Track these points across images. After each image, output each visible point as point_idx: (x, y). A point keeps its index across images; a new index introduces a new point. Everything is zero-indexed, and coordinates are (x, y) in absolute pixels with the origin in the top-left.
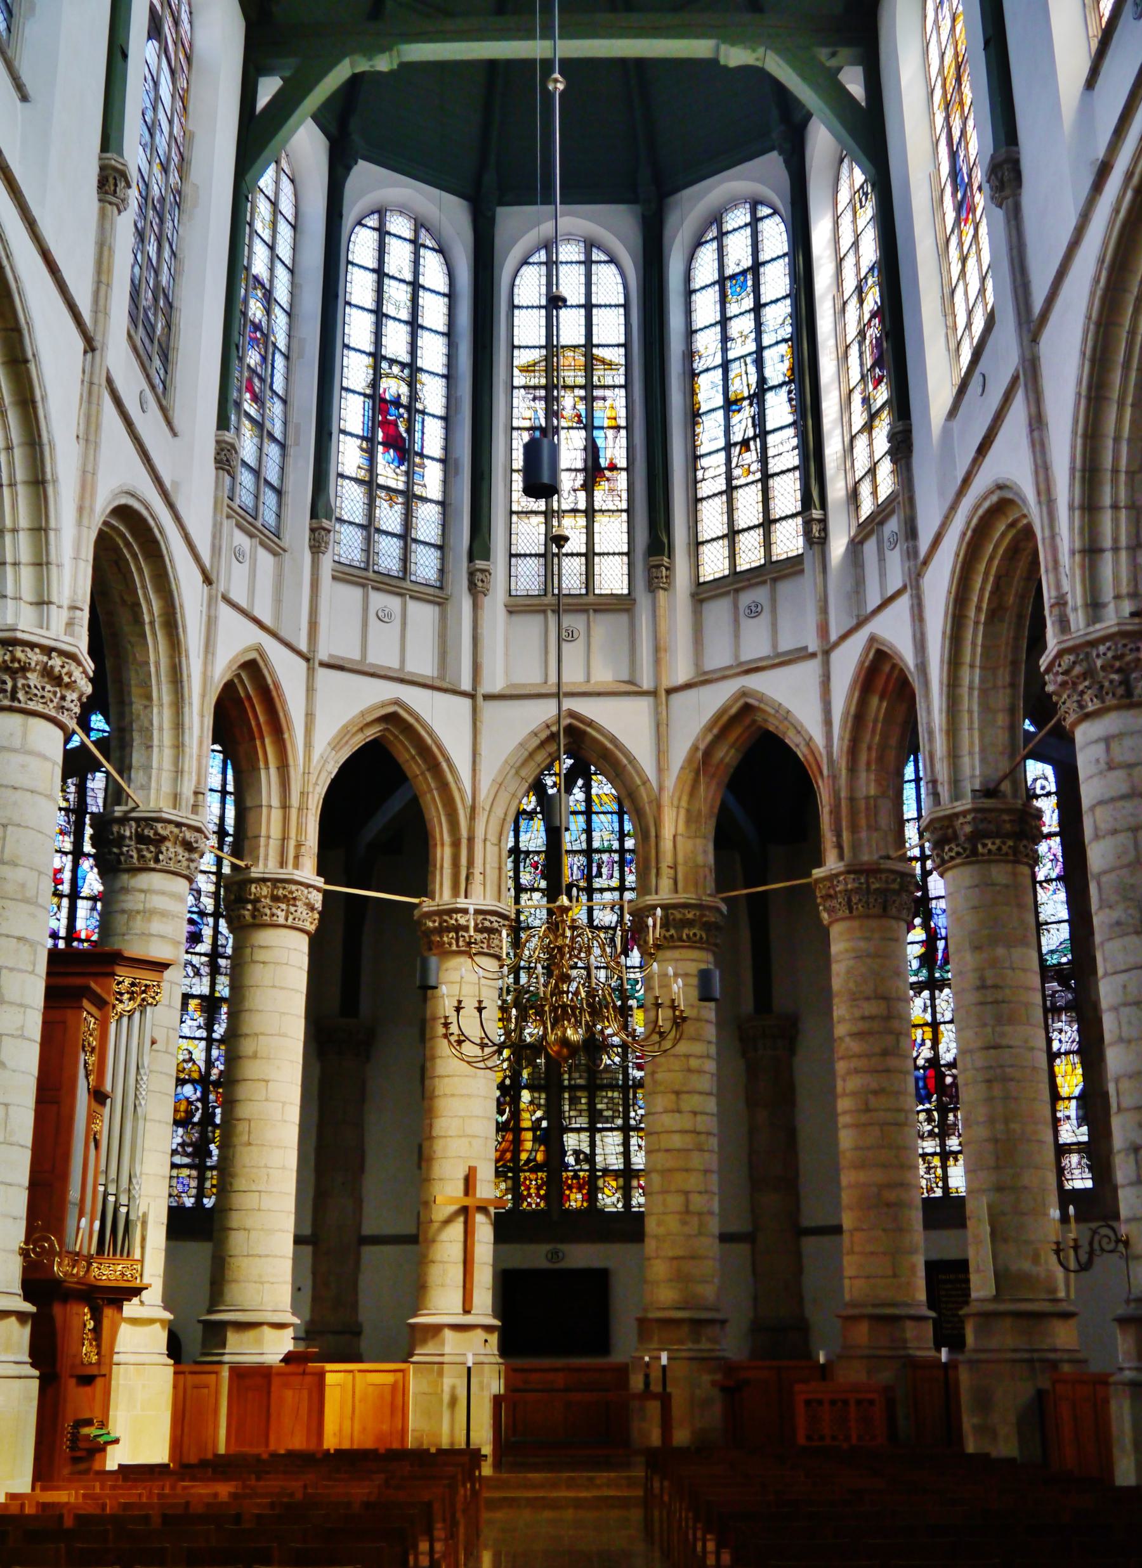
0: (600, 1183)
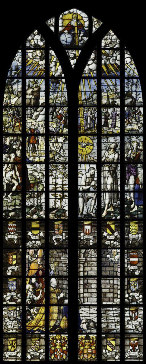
0: (104, 342)
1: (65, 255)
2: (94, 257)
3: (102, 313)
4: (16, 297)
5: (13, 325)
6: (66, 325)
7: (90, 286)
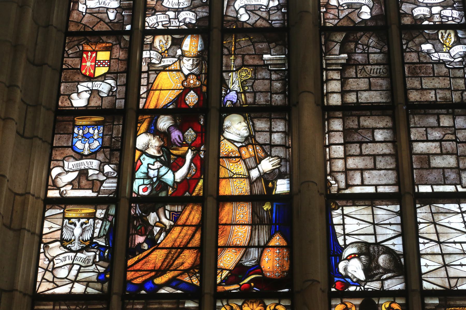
1: (277, 48)
2: (378, 51)
3: (419, 220)
4: (97, 172)
5: (76, 267)
6: (282, 266)
7: (370, 135)
